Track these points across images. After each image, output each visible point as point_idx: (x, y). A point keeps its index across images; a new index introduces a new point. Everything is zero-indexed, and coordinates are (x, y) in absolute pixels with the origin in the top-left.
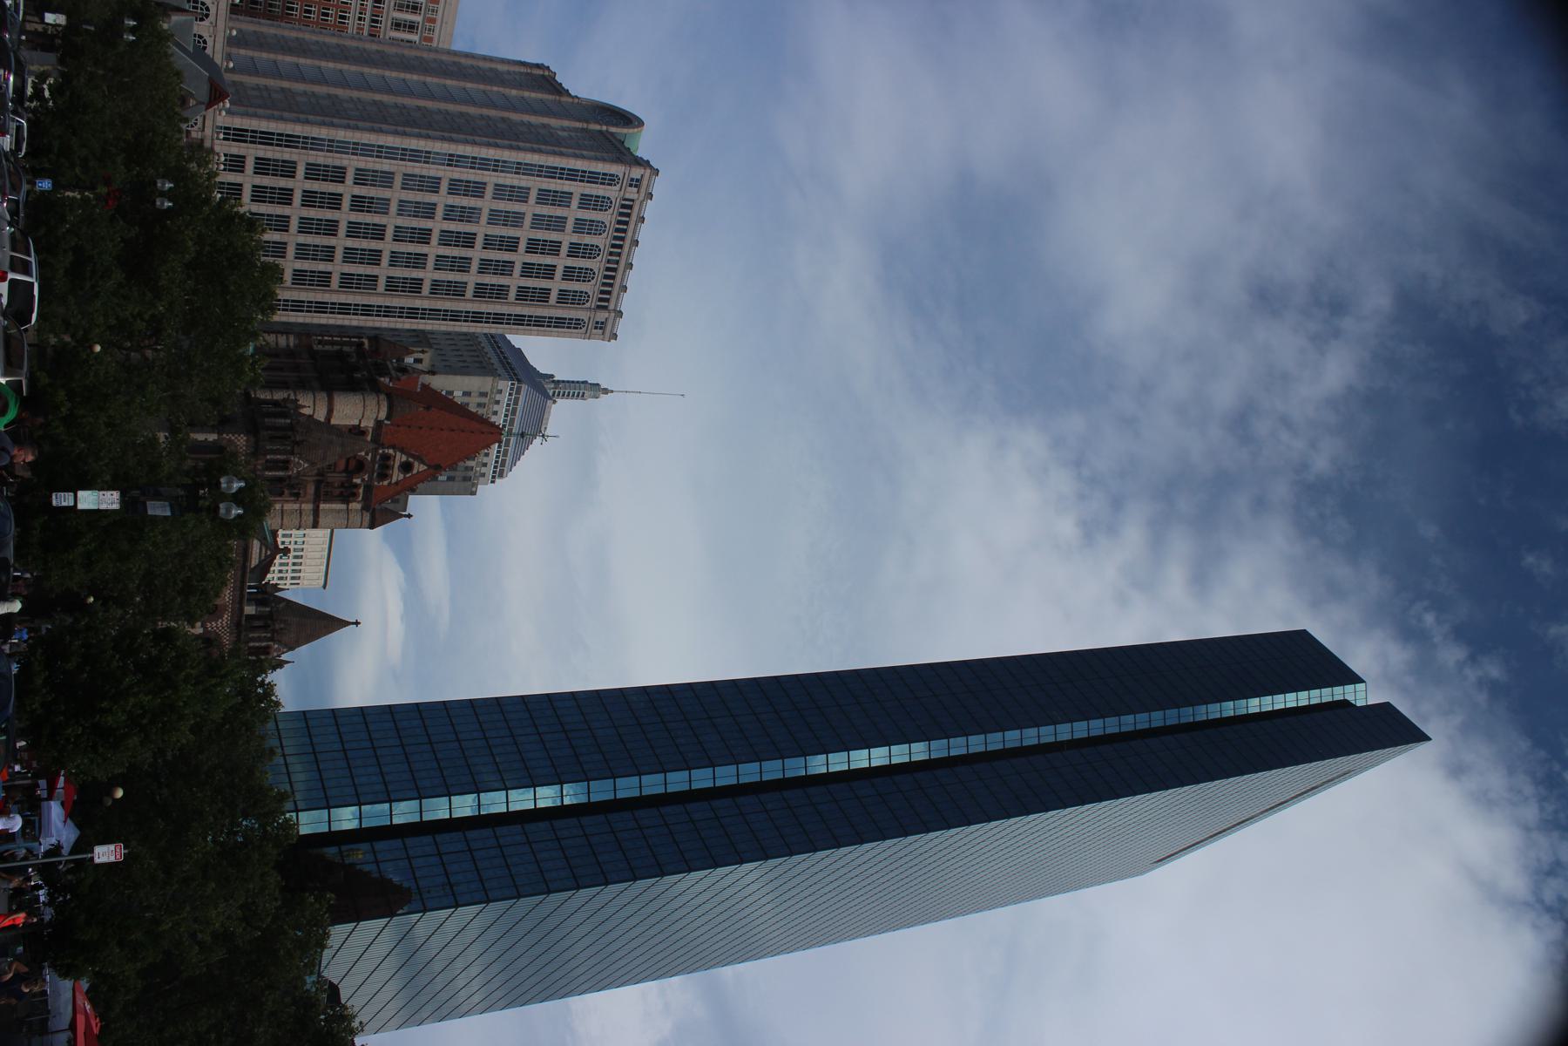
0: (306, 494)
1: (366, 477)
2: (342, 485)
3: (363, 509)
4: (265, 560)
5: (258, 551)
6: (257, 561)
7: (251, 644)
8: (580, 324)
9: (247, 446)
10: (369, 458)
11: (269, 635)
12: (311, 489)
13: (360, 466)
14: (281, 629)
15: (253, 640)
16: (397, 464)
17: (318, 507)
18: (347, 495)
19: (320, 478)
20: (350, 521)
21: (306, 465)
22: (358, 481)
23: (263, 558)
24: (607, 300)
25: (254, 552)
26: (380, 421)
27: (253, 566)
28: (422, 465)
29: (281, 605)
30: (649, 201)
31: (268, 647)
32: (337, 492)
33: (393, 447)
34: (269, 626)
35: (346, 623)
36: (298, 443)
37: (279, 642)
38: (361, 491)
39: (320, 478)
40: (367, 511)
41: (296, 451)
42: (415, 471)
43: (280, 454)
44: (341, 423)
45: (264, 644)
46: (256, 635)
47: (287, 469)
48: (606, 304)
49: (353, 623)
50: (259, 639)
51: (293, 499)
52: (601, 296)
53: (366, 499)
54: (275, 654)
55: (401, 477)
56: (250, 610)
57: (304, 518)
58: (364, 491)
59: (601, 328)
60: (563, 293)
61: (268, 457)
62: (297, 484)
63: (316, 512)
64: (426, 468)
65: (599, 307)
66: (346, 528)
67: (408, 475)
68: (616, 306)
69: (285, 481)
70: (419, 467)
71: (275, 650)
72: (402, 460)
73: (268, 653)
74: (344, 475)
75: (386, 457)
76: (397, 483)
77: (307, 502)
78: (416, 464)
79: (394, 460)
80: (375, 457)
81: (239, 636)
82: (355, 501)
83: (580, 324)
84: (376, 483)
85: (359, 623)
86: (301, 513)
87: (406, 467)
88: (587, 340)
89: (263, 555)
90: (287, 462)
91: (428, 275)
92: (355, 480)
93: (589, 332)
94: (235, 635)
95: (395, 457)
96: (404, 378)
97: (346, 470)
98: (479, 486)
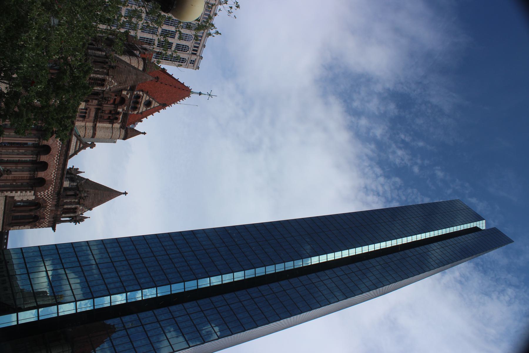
0: (89, 117)
1: (125, 108)
2: (110, 112)
3: (121, 127)
5: (75, 144)
6: (74, 151)
7: (66, 207)
8: (184, 61)
10: (128, 96)
11: (77, 200)
12: (93, 114)
13: (123, 101)
14: (85, 197)
15: (67, 203)
16: (143, 102)
17: (96, 125)
18: (112, 120)
19: (99, 107)
20: (113, 135)
21: (116, 84)
22: (120, 110)
23: (77, 149)
24: (196, 51)
25: (72, 145)
27: (70, 155)
29: (83, 182)
30: (219, 5)
31: (76, 208)
32: (106, 116)
33: (142, 91)
34: (78, 195)
35: (118, 194)
36: (113, 67)
37: (83, 205)
38: (121, 116)
39: (99, 107)
40: (123, 129)
41: (110, 74)
42: (152, 107)
43: (100, 74)
45: (73, 206)
46: (68, 201)
47: (103, 85)
48: (196, 52)
49: (123, 193)
50: (71, 203)
51: (81, 119)
52: (194, 48)
54: (80, 213)
55: (144, 109)
56: (66, 184)
57: (88, 131)
59: (193, 63)
60: (178, 45)
62: (108, 98)
63: (94, 128)
64: (158, 105)
65: (193, 54)
67: (148, 109)
68: (200, 53)
69: (100, 95)
70: (155, 104)
71: (80, 210)
72: (147, 99)
73: (75, 212)
74: (113, 106)
75: (138, 97)
76: (141, 113)
77: (89, 122)
78: (154, 102)
79: (142, 99)
80: (132, 96)
81: (58, 201)
82: (117, 122)
83: (184, 61)
84: (130, 112)
85: (127, 193)
86: (85, 128)
87: (148, 104)
88: (186, 68)
89: (78, 147)
90: (104, 80)
92: (119, 110)
93: (187, 65)
94: (56, 201)
95: (143, 97)
96: (146, 53)
97: (114, 103)
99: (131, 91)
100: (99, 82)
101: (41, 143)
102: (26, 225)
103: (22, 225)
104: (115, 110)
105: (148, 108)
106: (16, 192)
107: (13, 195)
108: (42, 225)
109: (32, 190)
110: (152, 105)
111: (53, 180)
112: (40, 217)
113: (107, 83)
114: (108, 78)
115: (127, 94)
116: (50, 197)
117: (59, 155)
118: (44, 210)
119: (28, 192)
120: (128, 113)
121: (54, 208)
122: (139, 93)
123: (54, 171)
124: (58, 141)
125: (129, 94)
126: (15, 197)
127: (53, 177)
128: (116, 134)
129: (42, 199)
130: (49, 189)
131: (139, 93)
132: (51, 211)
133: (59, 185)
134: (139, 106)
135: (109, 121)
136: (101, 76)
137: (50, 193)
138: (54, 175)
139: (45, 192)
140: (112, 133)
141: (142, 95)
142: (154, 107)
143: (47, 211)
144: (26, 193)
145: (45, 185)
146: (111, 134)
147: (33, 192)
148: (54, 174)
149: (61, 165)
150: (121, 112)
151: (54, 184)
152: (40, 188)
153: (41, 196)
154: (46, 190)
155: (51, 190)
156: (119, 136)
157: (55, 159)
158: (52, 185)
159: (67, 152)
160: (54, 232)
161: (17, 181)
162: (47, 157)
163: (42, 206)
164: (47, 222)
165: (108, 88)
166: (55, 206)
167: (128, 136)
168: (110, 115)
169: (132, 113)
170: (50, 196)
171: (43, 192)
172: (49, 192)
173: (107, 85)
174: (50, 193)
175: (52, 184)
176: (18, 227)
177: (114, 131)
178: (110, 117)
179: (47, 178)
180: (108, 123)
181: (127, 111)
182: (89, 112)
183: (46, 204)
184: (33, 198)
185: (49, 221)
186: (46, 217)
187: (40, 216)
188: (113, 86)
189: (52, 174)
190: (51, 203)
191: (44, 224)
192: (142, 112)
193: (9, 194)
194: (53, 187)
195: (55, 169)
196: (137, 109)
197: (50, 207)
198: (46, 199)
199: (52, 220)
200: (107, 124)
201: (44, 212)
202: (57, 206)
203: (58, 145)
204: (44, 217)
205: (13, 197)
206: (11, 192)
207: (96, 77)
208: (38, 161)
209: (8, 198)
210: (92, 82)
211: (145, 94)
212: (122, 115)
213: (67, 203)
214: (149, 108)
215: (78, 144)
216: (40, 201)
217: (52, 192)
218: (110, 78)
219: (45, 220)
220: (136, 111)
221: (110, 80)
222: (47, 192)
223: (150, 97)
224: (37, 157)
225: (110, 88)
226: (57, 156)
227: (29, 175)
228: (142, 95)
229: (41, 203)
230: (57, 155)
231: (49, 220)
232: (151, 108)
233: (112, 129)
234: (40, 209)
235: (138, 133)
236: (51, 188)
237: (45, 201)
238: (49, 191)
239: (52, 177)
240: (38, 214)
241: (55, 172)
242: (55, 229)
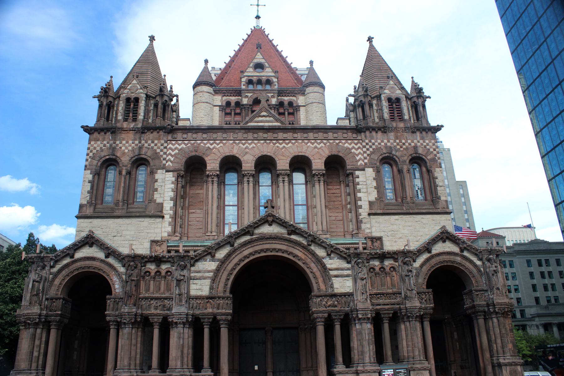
3: (303, 94)
4: (273, 116)
7: (386, 116)
9: (104, 140)
10: (250, 95)
15: (381, 118)
18: (293, 109)
20: (314, 101)
22: (274, 101)
23: (271, 119)
26: (214, 91)
28: (257, 57)
31: (389, 100)
38: (286, 99)
42: (263, 61)
44: (218, 119)
45: (385, 104)
46: (376, 115)
47: (137, 100)
50: (380, 110)
53: (293, 93)
55: (268, 70)
58: (285, 96)
61: (120, 117)
64: (259, 54)
66: (324, 104)
67: (267, 65)
70: (259, 58)
73: (398, 100)
75: (250, 82)
76: (276, 72)
78: (256, 61)
79: (252, 76)
82: (297, 102)
87: (259, 66)
89: (268, 119)
90: (128, 100)
98: (445, 148)
99: (241, 93)
100: (132, 105)
101: (251, 172)
102: (433, 175)
103: (435, 183)
104: (275, 108)
105: (266, 66)
106: (356, 200)
107: (367, 203)
108: (431, 150)
109: (352, 174)
110: (261, 61)
111: (328, 144)
112: (414, 155)
113: (133, 94)
114: (124, 95)
115: (247, 97)
116: (367, 144)
117: (274, 142)
118: (397, 150)
119: (357, 180)
120: (277, 89)
121: (392, 135)
123: (309, 144)
124: (247, 146)
125: (246, 94)
126: (370, 200)
127: (322, 144)
128: (313, 97)
129: (372, 156)
130: (350, 147)
131: (244, 83)
132: (397, 138)
133: (339, 133)
134: (263, 78)
135: (295, 113)
136: (120, 105)
137: (359, 145)
138: (319, 144)
139: (357, 152)
140: (312, 103)
141: (247, 77)
142: (264, 58)
143: (398, 144)
144: (360, 183)
145: (340, 154)
146: (314, 104)
147: (357, 173)
148: (316, 144)
149: (295, 135)
150: (278, 99)
151: (337, 141)
152: (347, 162)
153: (365, 158)
154: (351, 152)
155: (350, 144)
156: (316, 93)
157: (284, 147)
158: (340, 144)
159: (266, 129)
160: (442, 126)
161: (344, 203)
162: (279, 160)
163: (387, 155)
164: (424, 142)
165: (141, 91)
166: (385, 132)
167: (316, 80)
168: (286, 113)
169: (277, 85)
170: (364, 144)
171: (358, 155)
172: (356, 147)
173: (136, 93)
174: (359, 145)
175: (337, 144)
176: (438, 188)
177: (309, 102)
178: (289, 114)
179: (326, 153)
180: (298, 113)
181: (275, 92)
183: (382, 147)
184: (370, 172)
185: (422, 138)
186: (413, 144)
187: (411, 155)
188: (138, 85)
189: (316, 147)
190: (379, 141)
191: (428, 147)
192: (273, 72)
193: (364, 211)
194: (343, 141)
195: (305, 143)
196: (270, 78)
197: (388, 141)
198: (371, 150)
200: (301, 113)
201: (402, 149)
202: (384, 129)
203: (255, 146)
204: (412, 148)
205: (371, 203)
206: (361, 207)
207: (122, 111)
208: (289, 171)
209: (373, 212)
210: (133, 116)
211: (244, 75)
212: (283, 96)
213: (381, 118)
215: (260, 119)
216: (376, 158)
217: (356, 141)
218: (124, 92)
219: (420, 146)
220: (273, 80)
221: (128, 90)
222: (357, 149)
223: (249, 67)
224: (281, 174)
225: (141, 89)
226: (277, 144)
227: (322, 183)
228: (246, 78)
229: (381, 157)
230: (275, 144)
231: (419, 139)
232: (265, 62)
233: (307, 105)
234: (395, 157)
235: (311, 70)
236: (346, 145)
237: (378, 149)
238: (353, 148)
239: (323, 145)
240: (407, 159)
241: (311, 143)
242: (438, 126)
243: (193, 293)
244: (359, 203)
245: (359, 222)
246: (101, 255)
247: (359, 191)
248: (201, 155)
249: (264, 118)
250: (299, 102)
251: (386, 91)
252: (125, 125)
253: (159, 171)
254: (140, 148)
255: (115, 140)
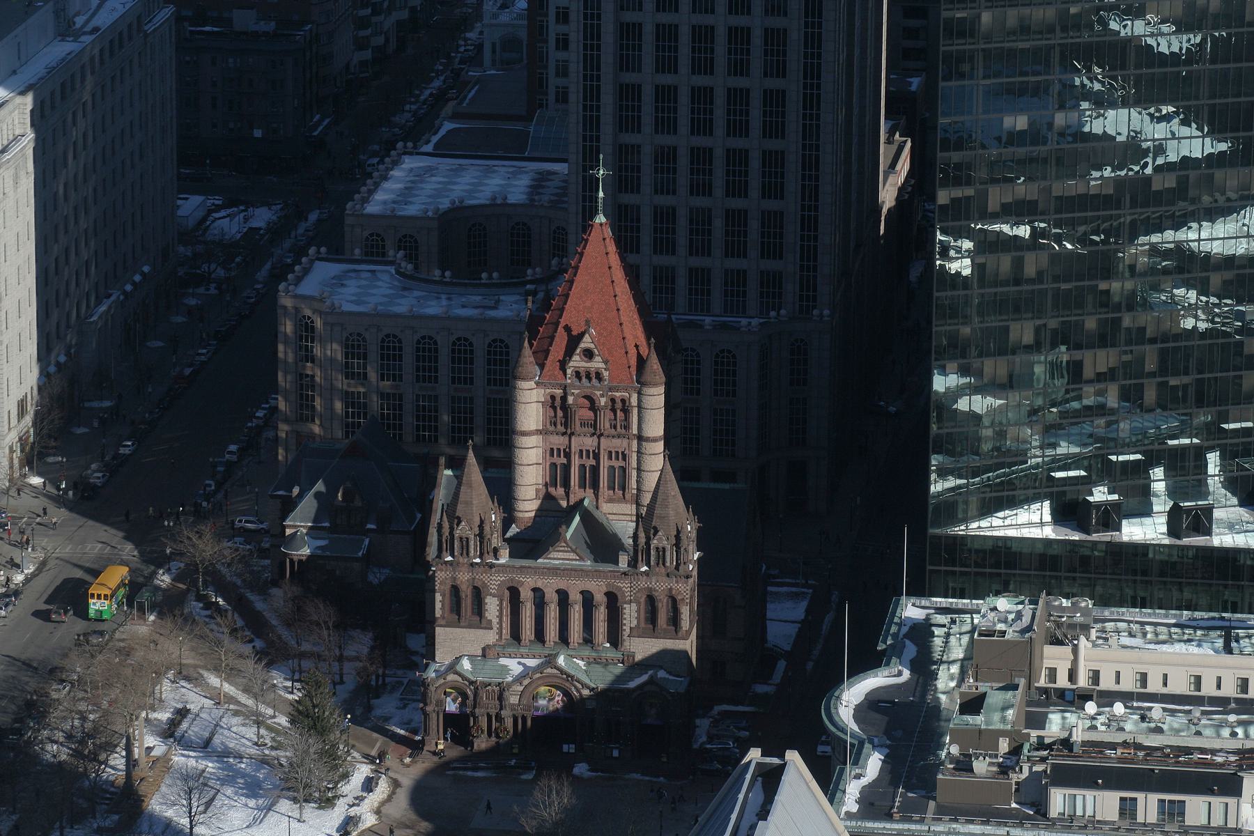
1: (598, 393)
9: (446, 570)
10: (576, 392)
22: (603, 401)
38: (618, 394)
42: (592, 346)
55: (598, 359)
76: (606, 362)
84: (606, 383)
91: (755, 82)
118: (655, 590)
122: (568, 376)
147: (625, 606)
179: (605, 589)
182: (615, 447)
184: (634, 607)
185: (677, 582)
199: (674, 579)
214: (596, 350)
243: (511, 702)
244: (624, 627)
245: (623, 641)
246: (460, 680)
247: (625, 619)
248: (516, 585)
249: (563, 549)
250: (632, 400)
251: (655, 541)
252: (461, 560)
253: (488, 597)
254: (474, 579)
255: (454, 570)
